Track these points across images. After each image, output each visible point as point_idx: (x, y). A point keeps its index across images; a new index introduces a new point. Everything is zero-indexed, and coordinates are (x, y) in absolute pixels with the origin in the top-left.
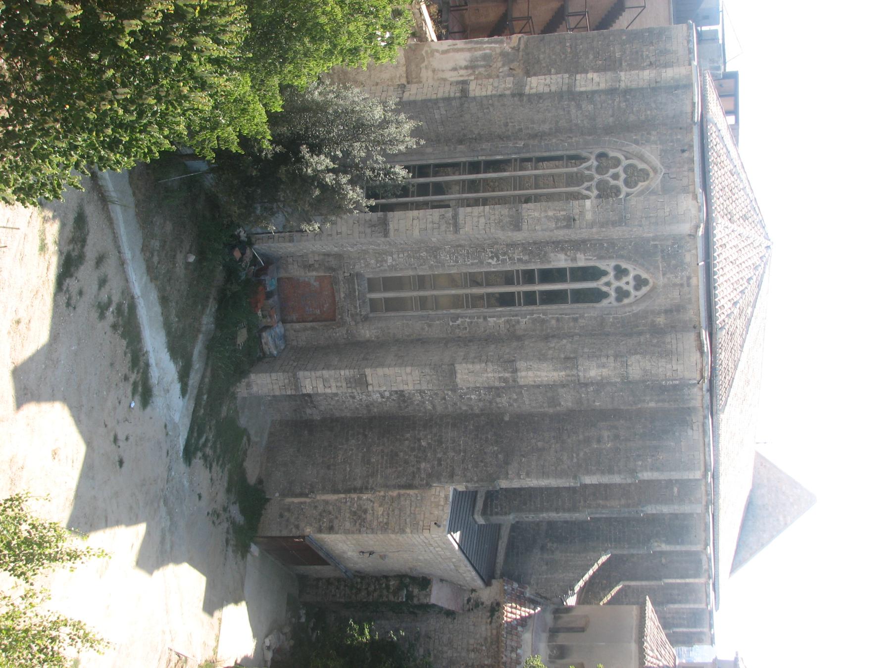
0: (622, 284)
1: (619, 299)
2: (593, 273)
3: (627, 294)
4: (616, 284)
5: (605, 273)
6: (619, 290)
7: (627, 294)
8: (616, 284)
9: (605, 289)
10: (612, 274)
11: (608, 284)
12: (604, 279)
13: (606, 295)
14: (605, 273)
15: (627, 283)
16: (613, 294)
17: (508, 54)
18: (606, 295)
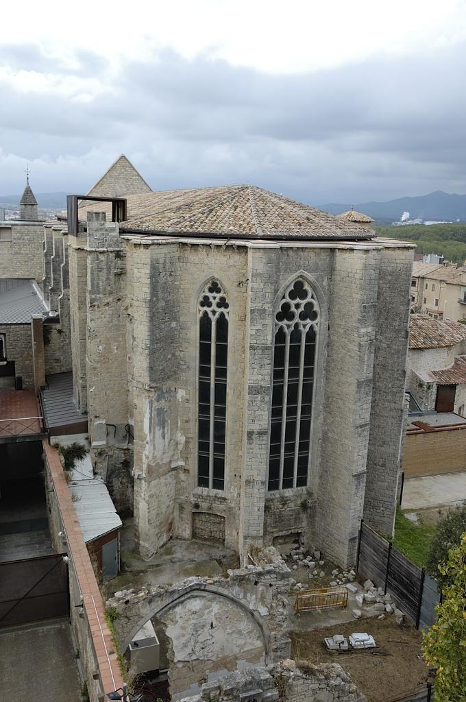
0: (214, 302)
1: (226, 306)
2: (205, 322)
3: (223, 299)
4: (214, 307)
5: (206, 313)
6: (219, 305)
7: (223, 299)
8: (214, 307)
9: (217, 315)
10: (206, 308)
11: (214, 312)
12: (210, 315)
13: (222, 315)
14: (206, 313)
15: (214, 298)
16: (222, 309)
17: (158, 395)
18: (222, 315)
